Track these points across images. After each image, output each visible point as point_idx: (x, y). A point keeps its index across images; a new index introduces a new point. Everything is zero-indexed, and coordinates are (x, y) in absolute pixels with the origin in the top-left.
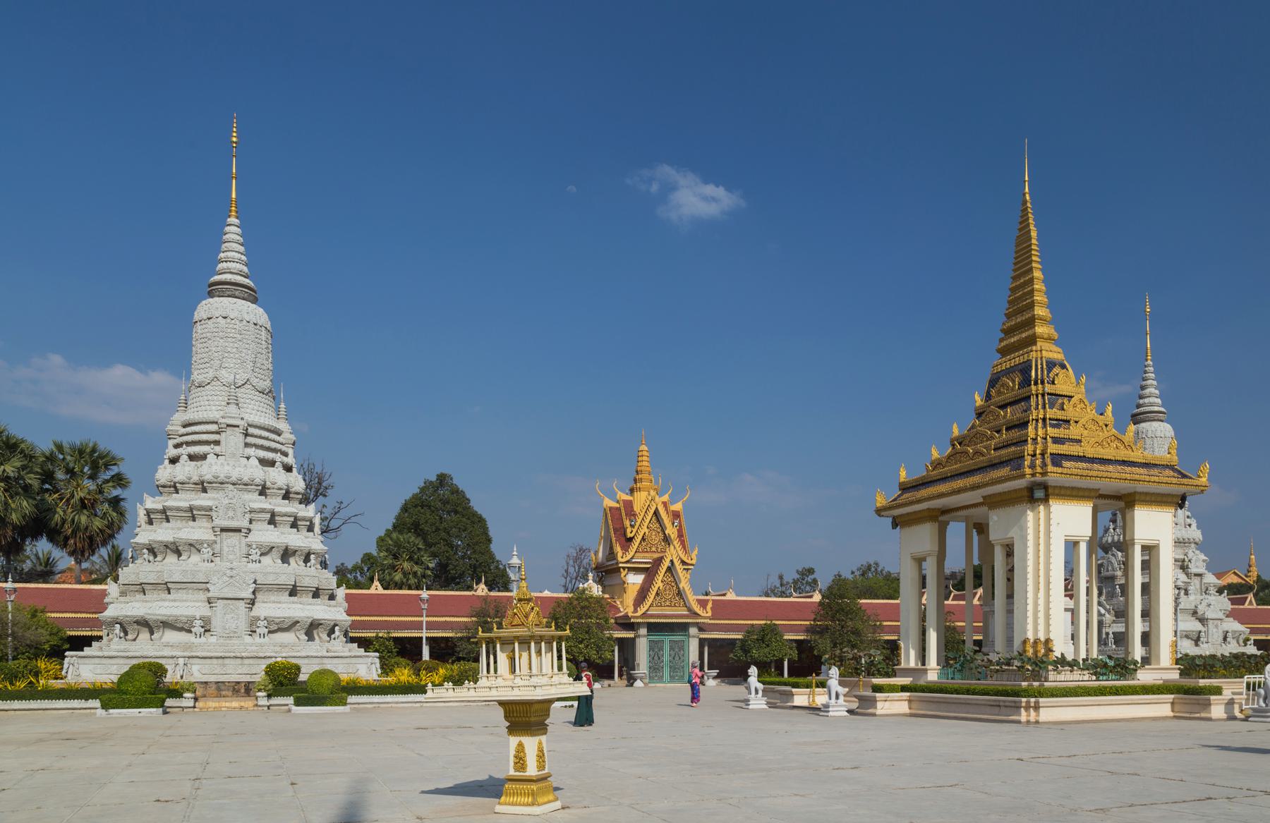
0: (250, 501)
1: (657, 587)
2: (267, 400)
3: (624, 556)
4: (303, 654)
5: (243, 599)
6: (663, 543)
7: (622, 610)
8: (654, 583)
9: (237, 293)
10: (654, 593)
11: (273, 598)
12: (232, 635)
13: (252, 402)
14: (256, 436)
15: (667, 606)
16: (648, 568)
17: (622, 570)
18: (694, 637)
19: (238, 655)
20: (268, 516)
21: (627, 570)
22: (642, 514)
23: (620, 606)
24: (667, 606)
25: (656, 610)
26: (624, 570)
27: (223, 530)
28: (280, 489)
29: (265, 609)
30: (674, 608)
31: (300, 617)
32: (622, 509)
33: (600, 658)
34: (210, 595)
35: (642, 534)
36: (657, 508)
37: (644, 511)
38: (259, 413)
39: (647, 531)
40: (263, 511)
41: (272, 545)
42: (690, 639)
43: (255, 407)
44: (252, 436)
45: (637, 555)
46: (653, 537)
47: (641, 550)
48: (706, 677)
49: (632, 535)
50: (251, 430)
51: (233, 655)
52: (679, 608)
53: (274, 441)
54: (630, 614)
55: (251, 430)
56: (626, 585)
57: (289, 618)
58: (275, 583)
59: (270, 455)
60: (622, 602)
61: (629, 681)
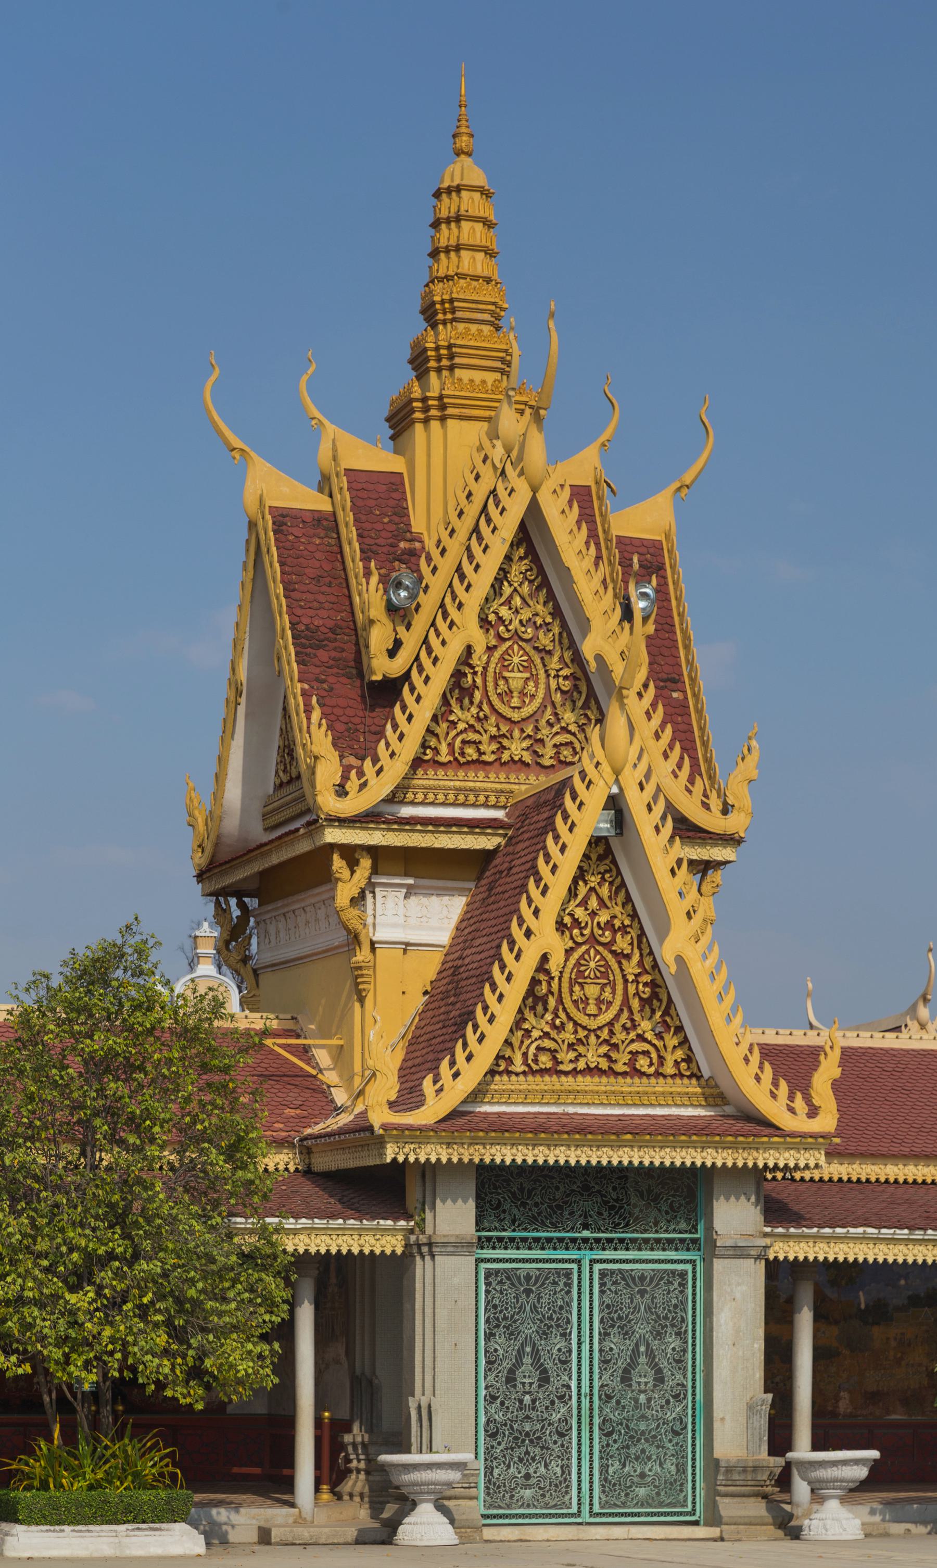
1: (531, 953)
3: (352, 785)
6: (569, 717)
7: (340, 1097)
8: (517, 933)
10: (515, 992)
15: (589, 1071)
16: (487, 856)
17: (338, 863)
18: (738, 1252)
21: (366, 863)
22: (455, 547)
23: (330, 1077)
24: (589, 1071)
25: (526, 1097)
26: (353, 864)
30: (625, 1085)
32: (347, 518)
33: (196, 1373)
35: (449, 657)
36: (534, 508)
37: (464, 527)
39: (480, 640)
42: (719, 1265)
45: (426, 779)
46: (516, 679)
47: (444, 757)
48: (801, 1488)
49: (395, 667)
54: (380, 1117)
56: (362, 955)
60: (341, 1055)
61: (376, 1509)
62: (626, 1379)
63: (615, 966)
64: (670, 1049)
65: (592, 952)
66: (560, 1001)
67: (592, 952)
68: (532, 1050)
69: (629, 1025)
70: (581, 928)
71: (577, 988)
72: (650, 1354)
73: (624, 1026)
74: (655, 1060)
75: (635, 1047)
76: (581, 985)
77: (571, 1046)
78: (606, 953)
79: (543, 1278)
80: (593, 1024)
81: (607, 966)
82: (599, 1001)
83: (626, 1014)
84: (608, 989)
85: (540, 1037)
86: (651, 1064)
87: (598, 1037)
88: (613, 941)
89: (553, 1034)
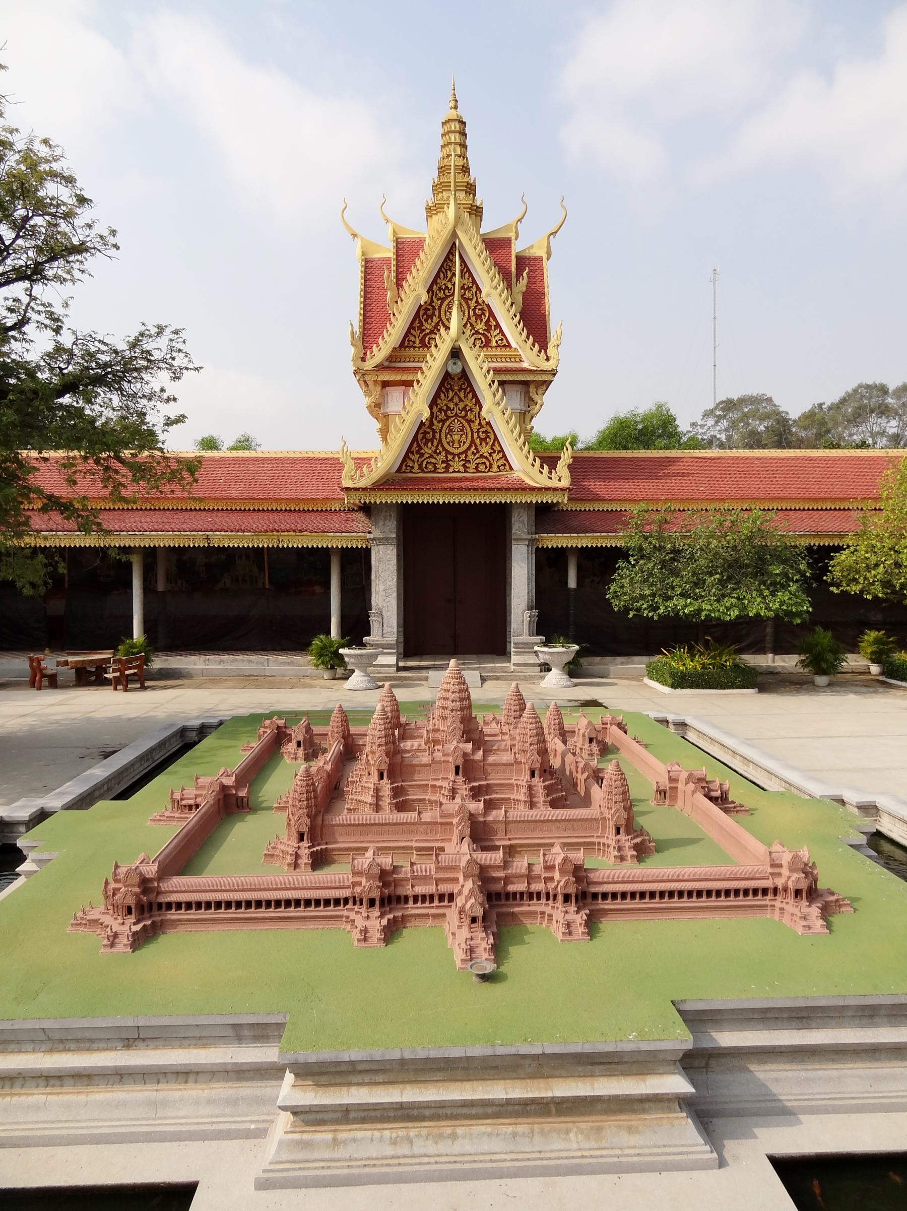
63: (467, 426)
64: (495, 461)
65: (456, 420)
66: (440, 442)
67: (456, 420)
68: (425, 463)
69: (475, 452)
70: (451, 411)
71: (449, 436)
73: (473, 453)
74: (488, 465)
75: (478, 461)
76: (450, 435)
78: (463, 421)
80: (456, 452)
81: (463, 426)
82: (459, 442)
83: (473, 447)
84: (464, 436)
85: (429, 457)
86: (486, 467)
87: (459, 458)
88: (466, 415)
89: (435, 456)
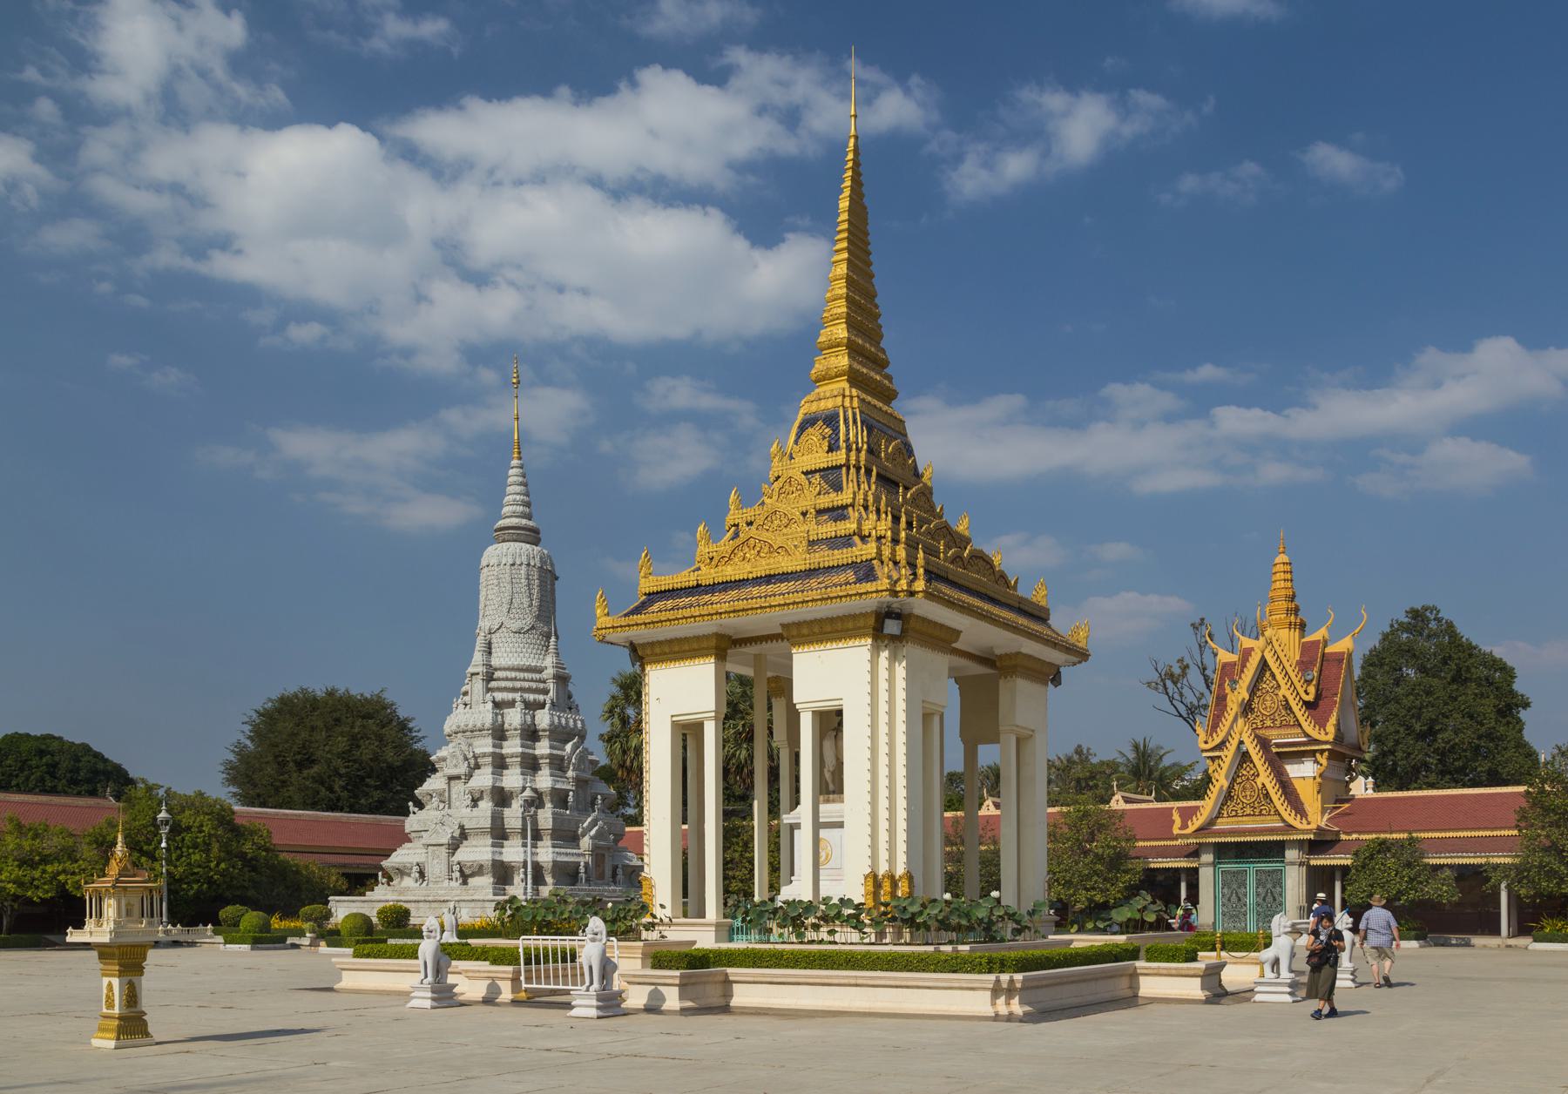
0: (480, 746)
2: (533, 637)
4: (470, 898)
5: (442, 845)
9: (506, 537)
11: (474, 843)
12: (438, 880)
13: (506, 645)
14: (503, 679)
15: (1247, 815)
19: (427, 899)
20: (490, 759)
24: (1247, 815)
27: (451, 778)
28: (515, 729)
29: (467, 854)
31: (482, 861)
34: (423, 841)
38: (510, 655)
40: (484, 755)
41: (482, 789)
43: (508, 649)
44: (498, 679)
50: (498, 674)
51: (423, 899)
52: (1269, 818)
53: (524, 680)
55: (498, 674)
57: (475, 861)
58: (478, 826)
59: (509, 696)
62: (1264, 900)
72: (1272, 892)
77: (1242, 809)
79: (1238, 872)
